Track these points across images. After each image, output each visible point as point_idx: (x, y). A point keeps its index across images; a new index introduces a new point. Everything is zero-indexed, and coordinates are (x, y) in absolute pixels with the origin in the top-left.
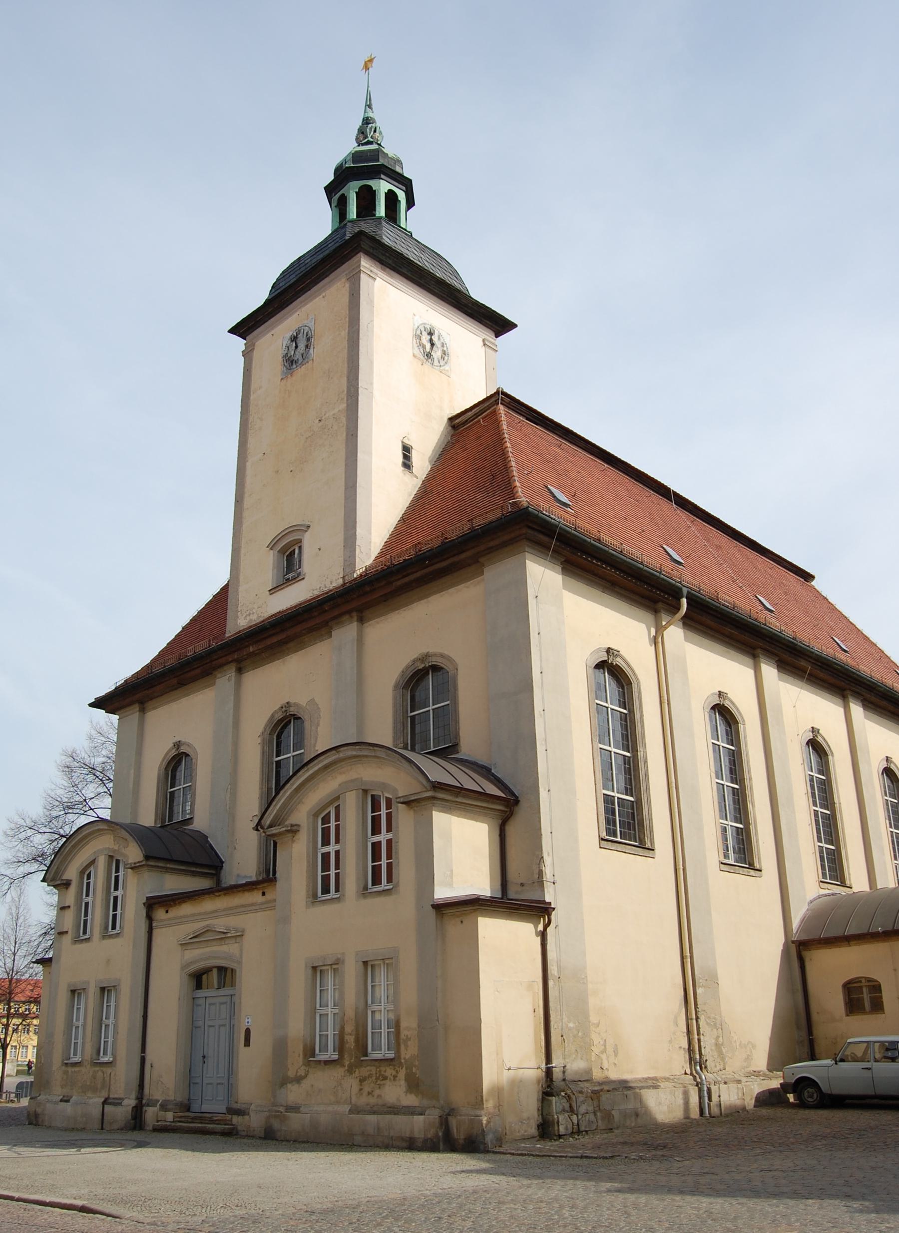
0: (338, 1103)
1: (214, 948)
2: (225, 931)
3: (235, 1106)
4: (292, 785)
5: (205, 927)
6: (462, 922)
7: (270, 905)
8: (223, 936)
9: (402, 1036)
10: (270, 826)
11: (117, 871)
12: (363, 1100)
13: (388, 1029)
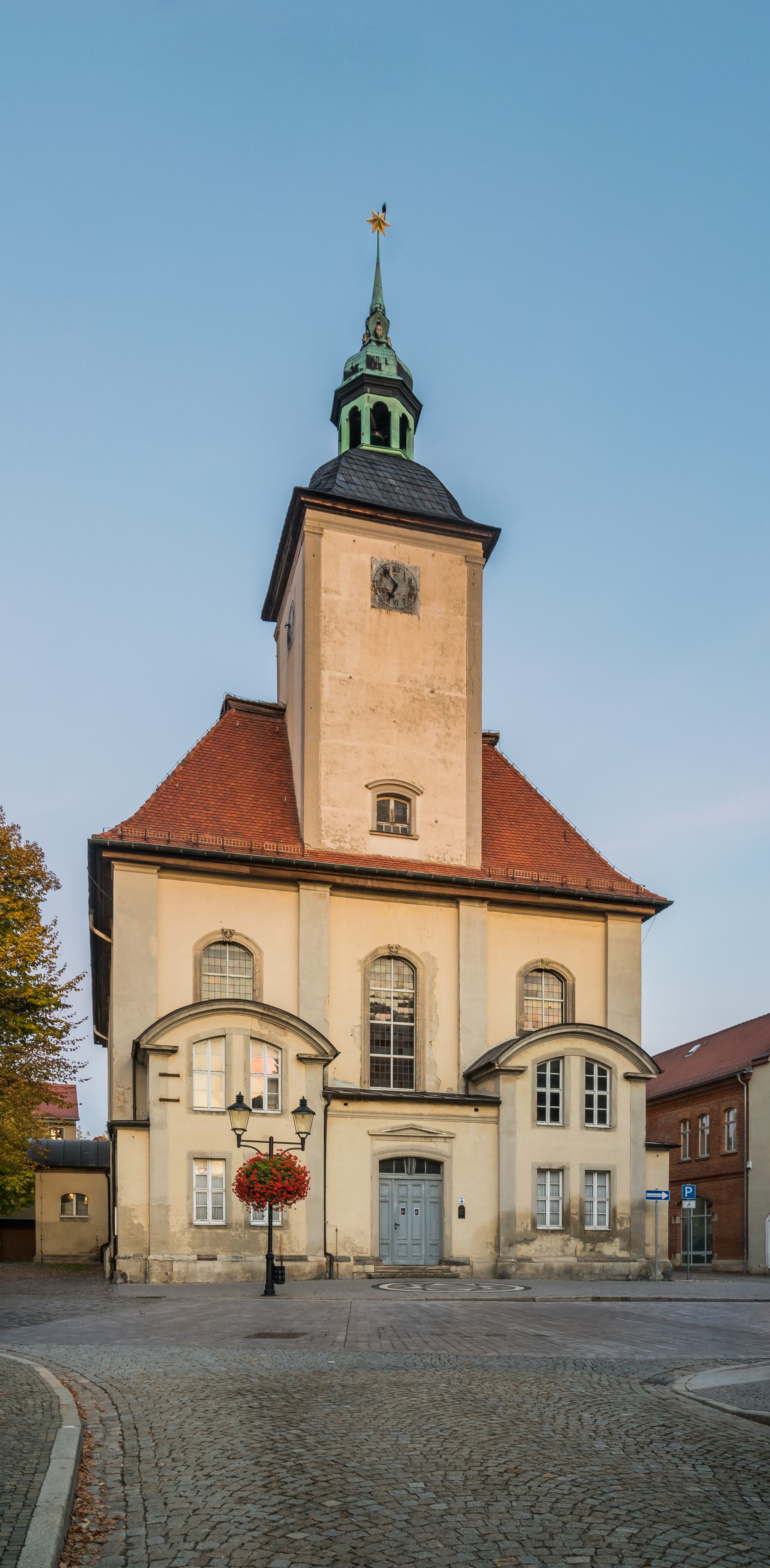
0: (565, 1255)
8: (434, 1135)
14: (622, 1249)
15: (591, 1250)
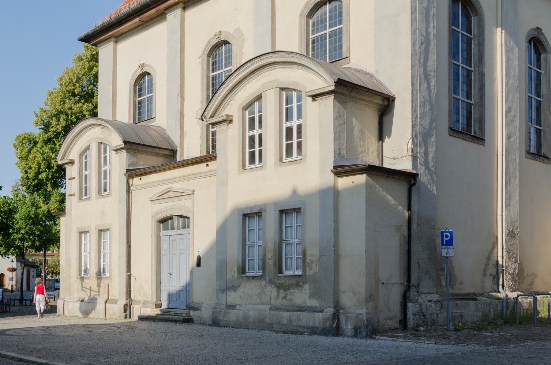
0: (262, 303)
1: (174, 203)
2: (181, 191)
3: (192, 305)
4: (227, 86)
5: (167, 189)
6: (353, 182)
7: (212, 174)
9: (308, 260)
10: (212, 117)
11: (105, 152)
12: (279, 302)
13: (297, 256)
14: (312, 296)
15: (285, 298)
